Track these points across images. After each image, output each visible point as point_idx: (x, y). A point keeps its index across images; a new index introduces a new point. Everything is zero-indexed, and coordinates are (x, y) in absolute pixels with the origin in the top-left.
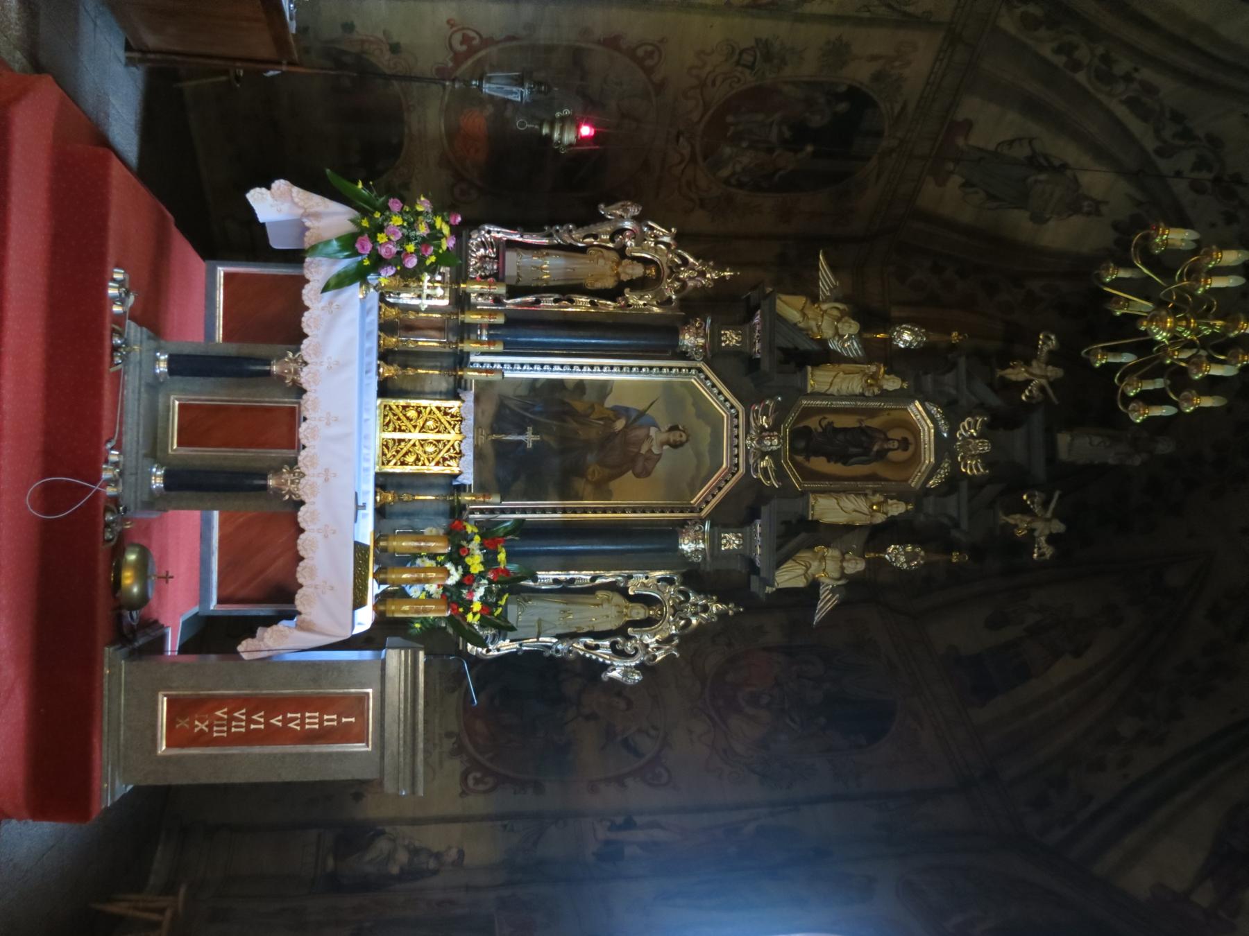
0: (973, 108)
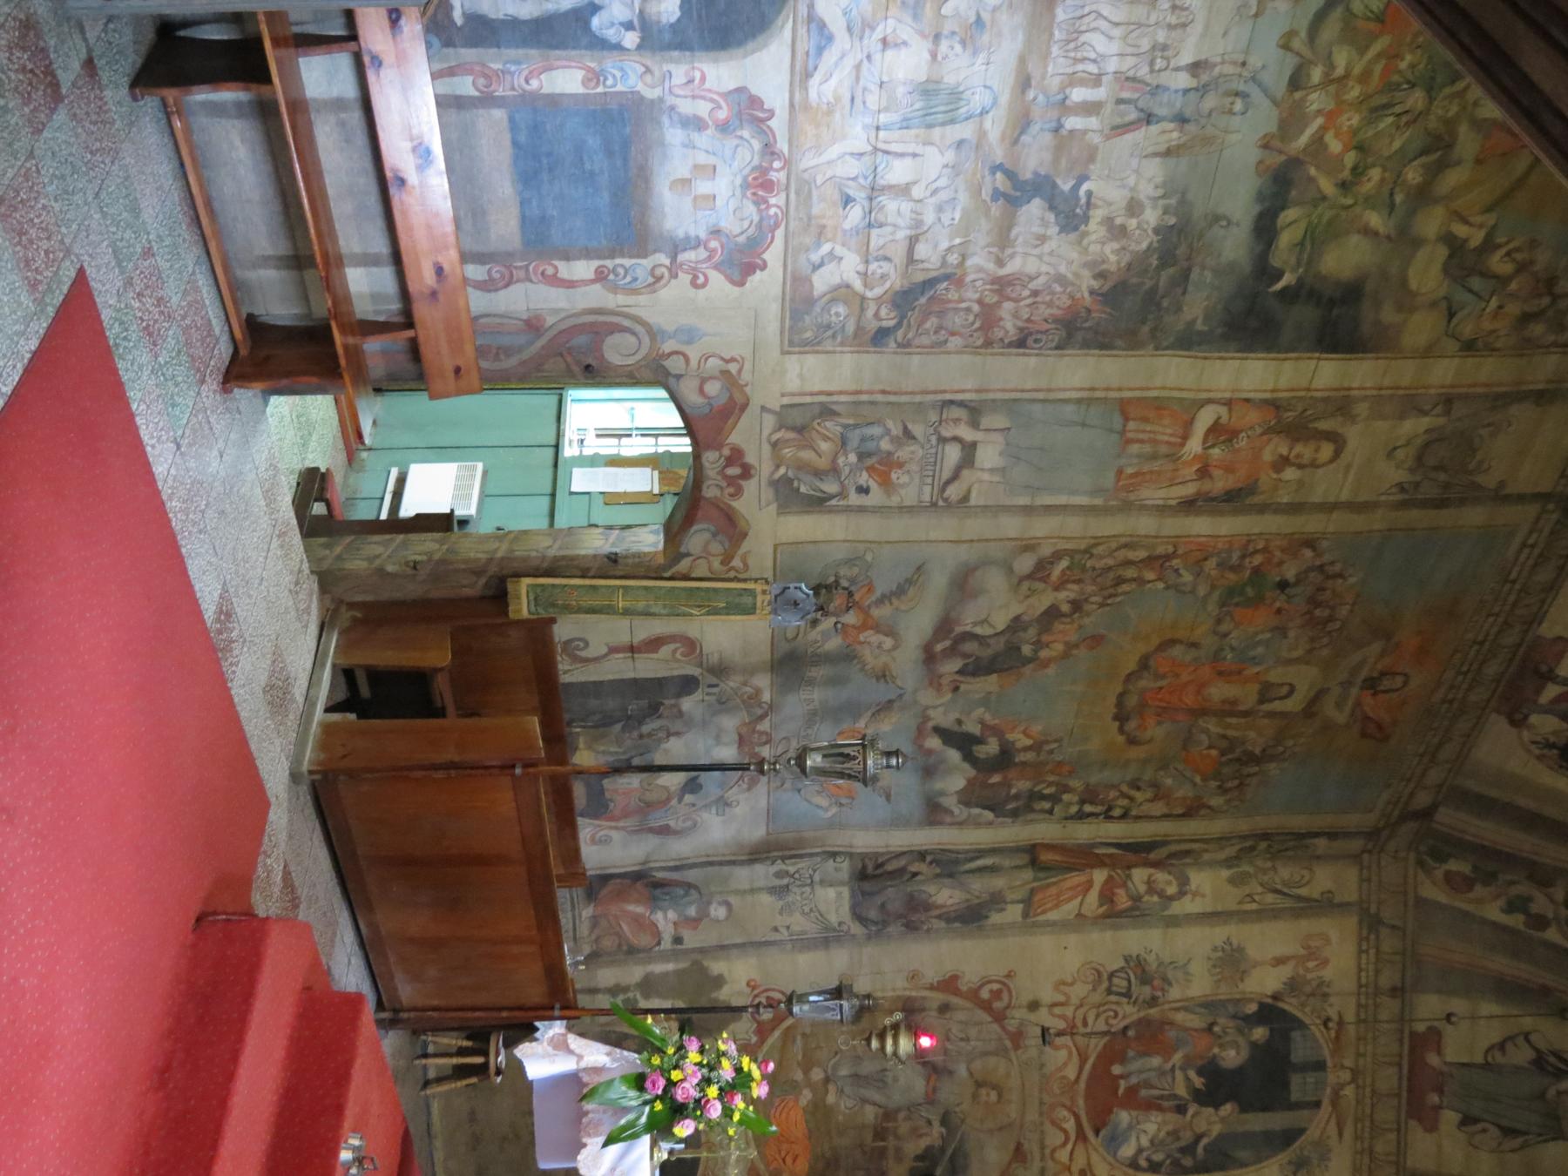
0: (1429, 1006)
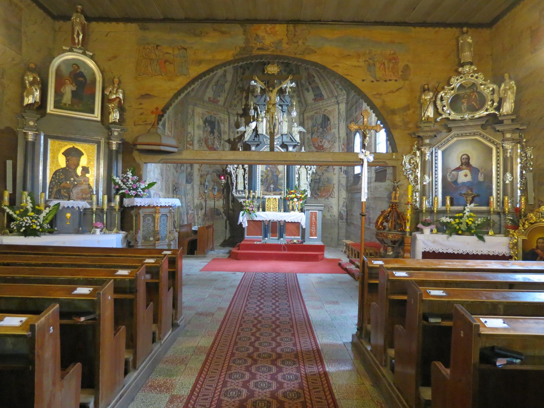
0: (206, 98)
